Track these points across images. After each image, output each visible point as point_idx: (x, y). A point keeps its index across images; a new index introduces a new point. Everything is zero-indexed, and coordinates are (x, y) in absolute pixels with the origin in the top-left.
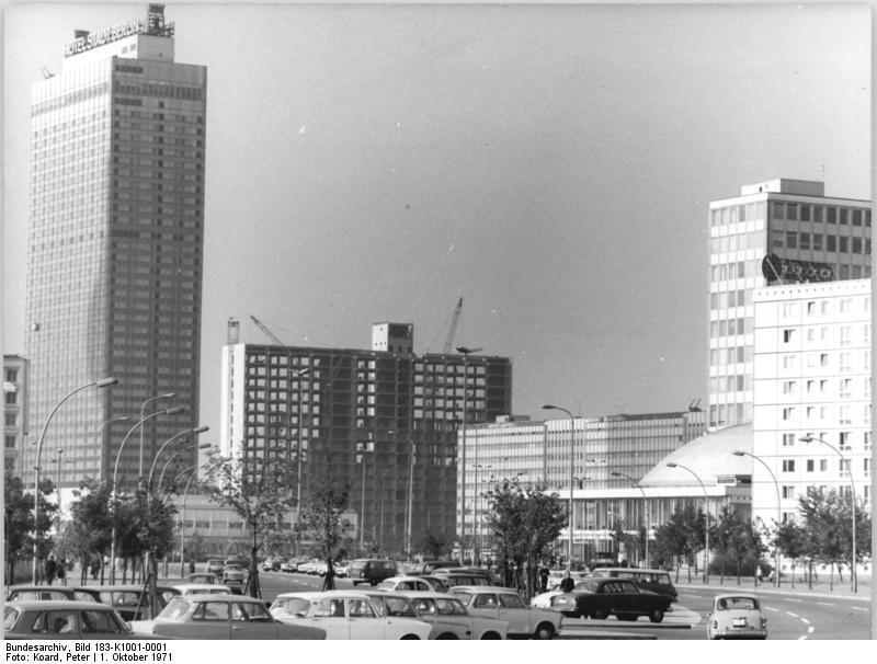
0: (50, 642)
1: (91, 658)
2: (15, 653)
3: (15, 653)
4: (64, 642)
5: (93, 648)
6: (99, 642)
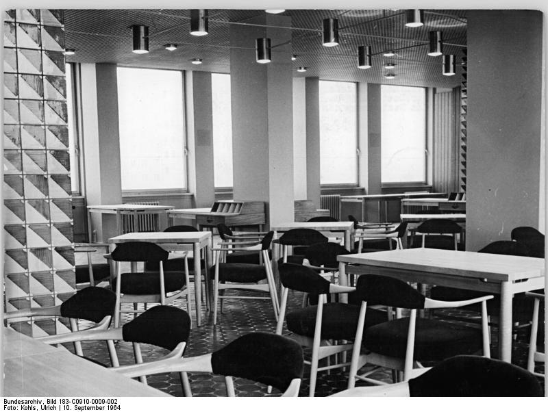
0: (31, 399)
1: (58, 408)
2: (10, 405)
3: (10, 405)
4: (40, 399)
5: (58, 401)
6: (62, 398)
